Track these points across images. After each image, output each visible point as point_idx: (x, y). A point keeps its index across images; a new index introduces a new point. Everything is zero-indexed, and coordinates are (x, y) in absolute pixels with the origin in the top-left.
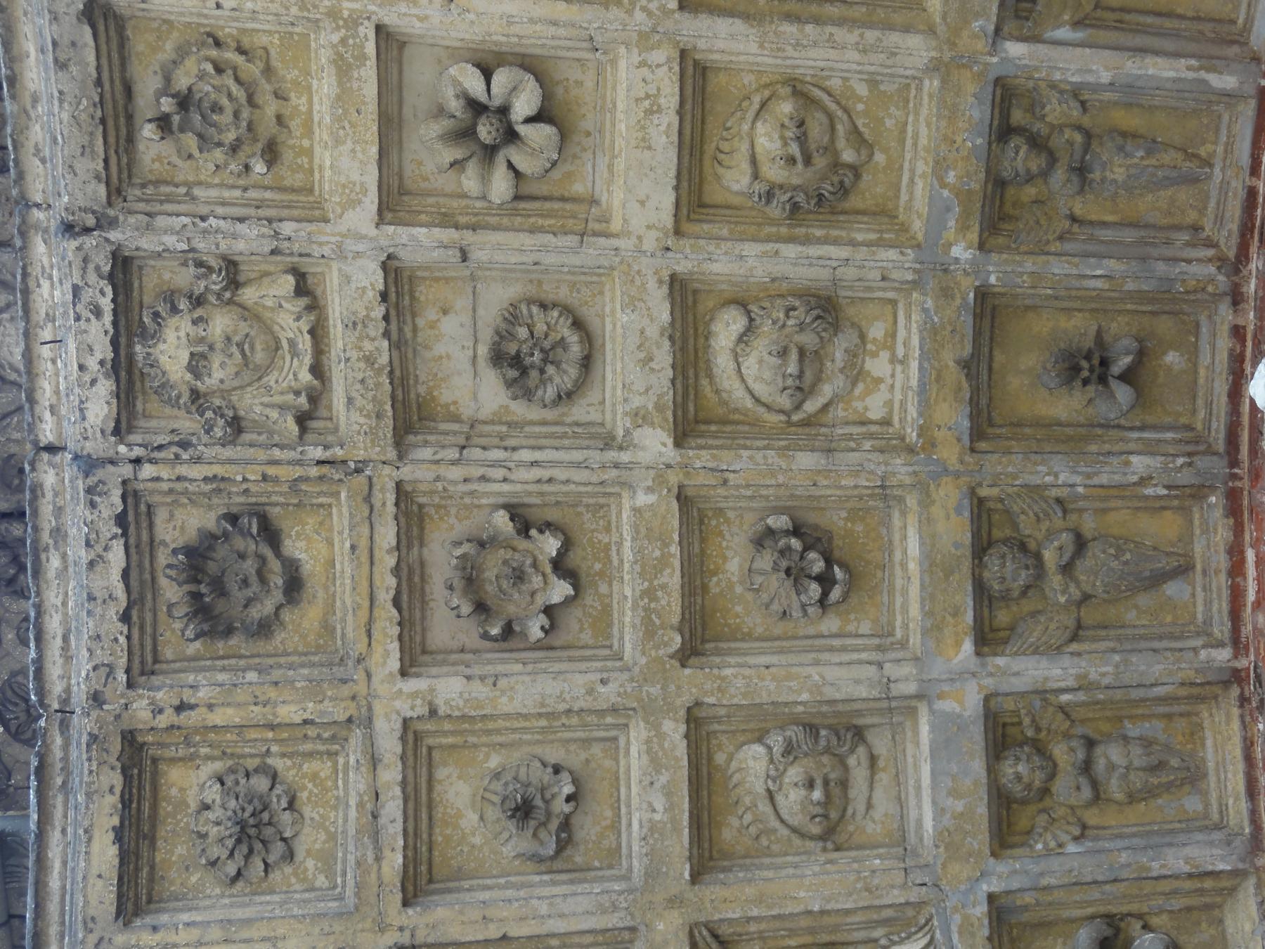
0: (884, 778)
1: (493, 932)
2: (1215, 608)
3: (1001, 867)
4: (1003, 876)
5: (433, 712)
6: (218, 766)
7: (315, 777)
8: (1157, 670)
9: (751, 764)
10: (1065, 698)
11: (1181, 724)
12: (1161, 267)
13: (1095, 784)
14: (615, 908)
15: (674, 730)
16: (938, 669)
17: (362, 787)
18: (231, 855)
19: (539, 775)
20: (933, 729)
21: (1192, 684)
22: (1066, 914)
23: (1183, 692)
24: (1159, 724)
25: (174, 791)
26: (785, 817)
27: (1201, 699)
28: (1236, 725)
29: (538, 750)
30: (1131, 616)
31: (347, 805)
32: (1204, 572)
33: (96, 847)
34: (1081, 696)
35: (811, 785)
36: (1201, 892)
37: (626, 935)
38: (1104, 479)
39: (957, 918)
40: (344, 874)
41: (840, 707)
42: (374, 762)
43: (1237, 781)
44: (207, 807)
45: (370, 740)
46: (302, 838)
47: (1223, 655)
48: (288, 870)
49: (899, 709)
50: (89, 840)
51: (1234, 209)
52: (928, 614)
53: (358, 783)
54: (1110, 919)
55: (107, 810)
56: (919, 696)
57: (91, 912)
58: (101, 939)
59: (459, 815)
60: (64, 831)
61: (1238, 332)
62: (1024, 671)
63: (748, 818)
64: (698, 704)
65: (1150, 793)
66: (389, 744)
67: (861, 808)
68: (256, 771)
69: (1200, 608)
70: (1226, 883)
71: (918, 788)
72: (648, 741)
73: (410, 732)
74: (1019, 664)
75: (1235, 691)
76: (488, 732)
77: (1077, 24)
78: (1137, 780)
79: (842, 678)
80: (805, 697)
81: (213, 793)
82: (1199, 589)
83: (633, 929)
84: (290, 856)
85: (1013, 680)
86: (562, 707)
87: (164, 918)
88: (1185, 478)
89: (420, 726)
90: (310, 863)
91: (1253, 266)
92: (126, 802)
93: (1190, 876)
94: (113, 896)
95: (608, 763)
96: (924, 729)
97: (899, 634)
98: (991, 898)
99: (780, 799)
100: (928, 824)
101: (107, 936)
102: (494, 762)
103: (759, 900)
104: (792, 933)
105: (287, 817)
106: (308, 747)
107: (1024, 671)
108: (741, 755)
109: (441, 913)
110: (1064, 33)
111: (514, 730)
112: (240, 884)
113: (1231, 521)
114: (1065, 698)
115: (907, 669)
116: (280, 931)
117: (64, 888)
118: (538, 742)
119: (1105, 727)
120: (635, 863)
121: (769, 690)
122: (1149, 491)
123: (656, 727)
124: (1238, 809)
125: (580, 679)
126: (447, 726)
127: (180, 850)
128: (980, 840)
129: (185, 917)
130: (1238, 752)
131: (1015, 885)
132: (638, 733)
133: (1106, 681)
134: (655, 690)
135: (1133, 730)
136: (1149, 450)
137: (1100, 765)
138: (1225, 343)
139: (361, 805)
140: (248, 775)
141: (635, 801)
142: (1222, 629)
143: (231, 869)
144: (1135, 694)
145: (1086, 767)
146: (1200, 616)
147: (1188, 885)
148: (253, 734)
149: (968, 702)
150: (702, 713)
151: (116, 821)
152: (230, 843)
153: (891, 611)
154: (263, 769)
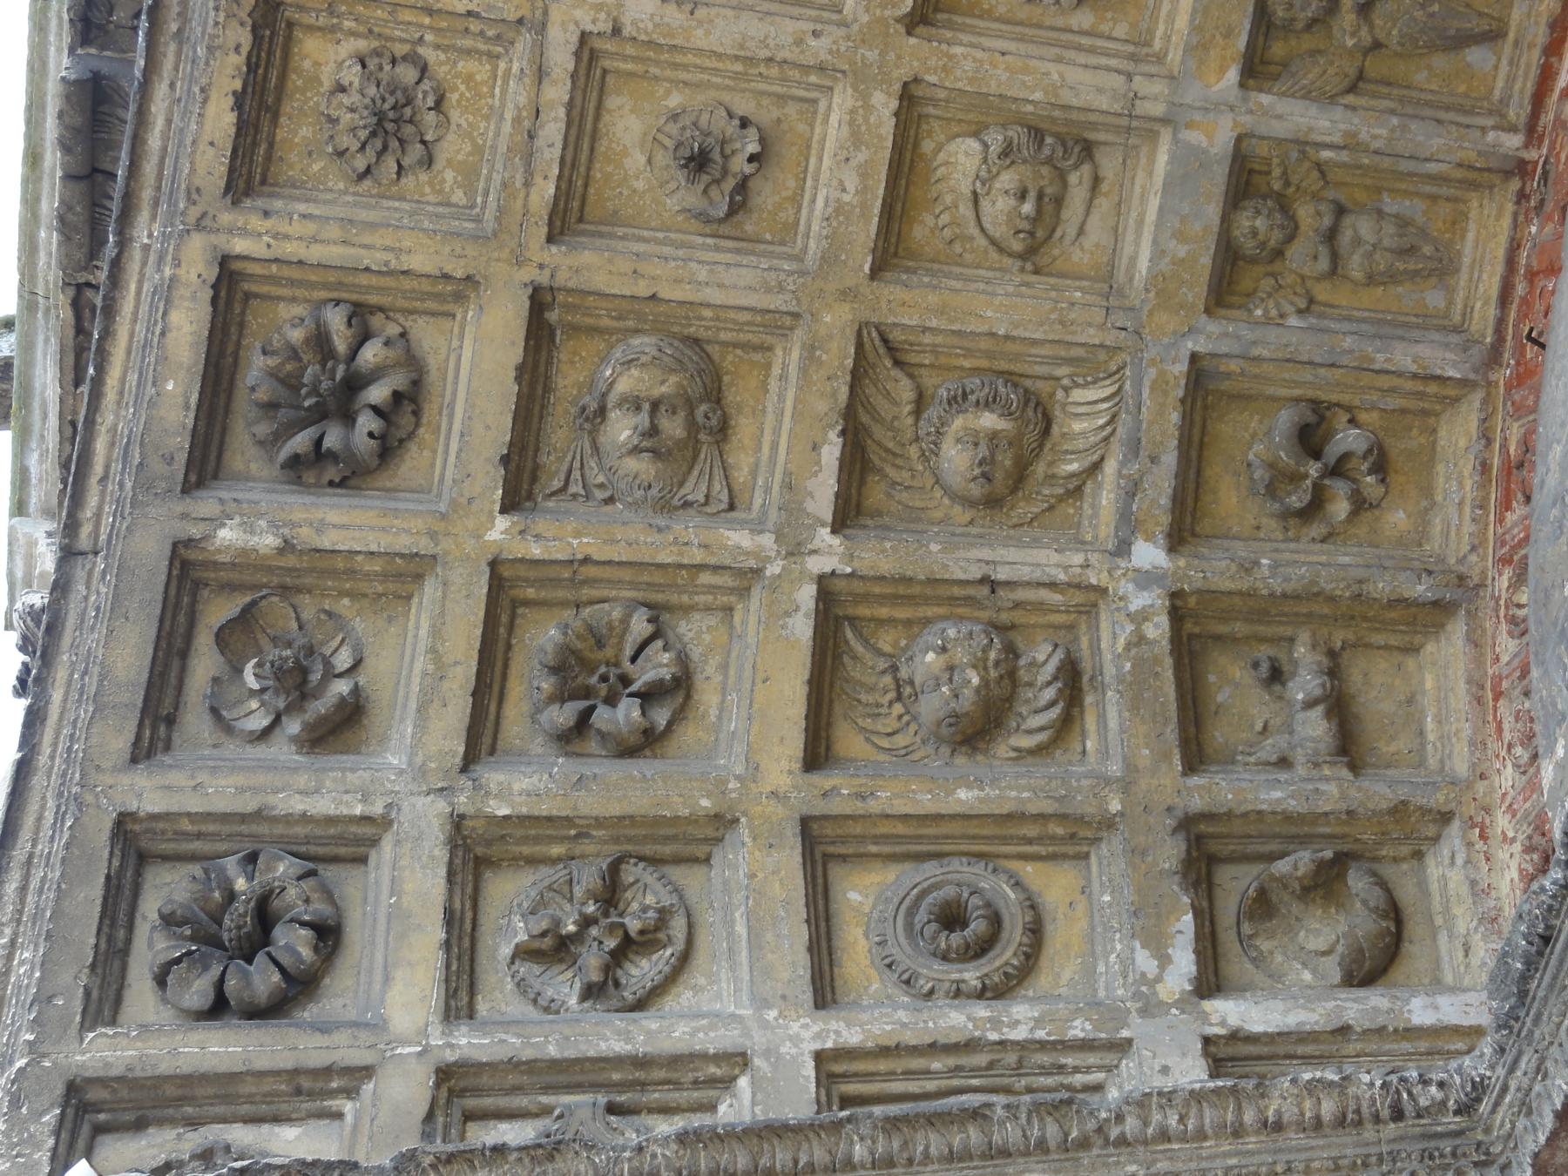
0: (1103, 204)
1: (642, 289)
2: (1517, 87)
3: (1213, 327)
4: (1213, 336)
5: (616, 31)
6: (362, 45)
7: (469, 78)
8: (1437, 144)
9: (959, 159)
11: (1445, 209)
13: (1335, 257)
14: (781, 288)
15: (884, 105)
16: (1192, 94)
17: (522, 100)
18: (363, 147)
19: (722, 125)
20: (1173, 159)
21: (1471, 167)
22: (1270, 391)
23: (1459, 174)
24: (1420, 205)
25: (307, 64)
26: (987, 225)
27: (1474, 186)
28: (1506, 222)
29: (726, 97)
30: (1420, 77)
31: (502, 117)
32: (1516, 43)
33: (211, 109)
34: (1344, 156)
35: (1022, 196)
36: (1421, 395)
37: (788, 321)
39: (1152, 373)
40: (486, 194)
41: (1074, 116)
42: (541, 74)
43: (1491, 284)
44: (342, 89)
45: (540, 49)
46: (444, 144)
47: (1512, 142)
48: (424, 177)
49: (1138, 129)
50: (205, 101)
52: (1196, 29)
53: (518, 94)
54: (1316, 405)
55: (230, 71)
56: (1165, 121)
57: (197, 182)
58: (204, 215)
59: (625, 153)
60: (172, 85)
62: (1288, 115)
63: (945, 218)
64: (916, 80)
65: (1392, 278)
66: (561, 59)
67: (1072, 232)
68: (404, 58)
69: (1500, 84)
70: (1452, 392)
71: (1140, 223)
72: (852, 112)
73: (586, 50)
74: (1284, 106)
75: (1515, 184)
76: (675, 66)
78: (1382, 261)
79: (1085, 85)
80: (1038, 96)
81: (352, 75)
82: (1504, 62)
83: (796, 316)
84: (428, 161)
85: (1274, 122)
86: (764, 53)
87: (278, 204)
89: (598, 44)
90: (449, 175)
92: (252, 66)
93: (1415, 376)
94: (224, 169)
95: (802, 127)
96: (1162, 158)
97: (1157, 44)
98: (1194, 358)
99: (985, 204)
100: (1143, 264)
101: (211, 212)
102: (675, 101)
103: (941, 311)
104: (969, 353)
105: (431, 117)
106: (467, 43)
107: (1288, 115)
108: (952, 147)
109: (587, 257)
111: (704, 69)
112: (367, 183)
114: (1326, 154)
115: (1158, 87)
116: (407, 244)
117: (164, 149)
118: (728, 88)
119: (1360, 196)
120: (812, 244)
121: (999, 79)
123: (865, 97)
124: (1484, 316)
125: (790, 26)
126: (630, 50)
127: (305, 132)
128: (1196, 292)
129: (302, 207)
130: (1501, 253)
131: (1224, 349)
132: (842, 100)
133: (1376, 145)
134: (872, 55)
135: (1390, 205)
137: (1346, 237)
139: (517, 120)
140: (394, 62)
141: (825, 175)
142: (1518, 111)
143: (360, 164)
144: (1406, 166)
145: (1331, 236)
146: (1497, 94)
147: (1409, 385)
148: (407, 16)
149: (1218, 138)
150: (919, 91)
151: (238, 85)
152: (363, 134)
153: (1154, 17)
154: (412, 58)
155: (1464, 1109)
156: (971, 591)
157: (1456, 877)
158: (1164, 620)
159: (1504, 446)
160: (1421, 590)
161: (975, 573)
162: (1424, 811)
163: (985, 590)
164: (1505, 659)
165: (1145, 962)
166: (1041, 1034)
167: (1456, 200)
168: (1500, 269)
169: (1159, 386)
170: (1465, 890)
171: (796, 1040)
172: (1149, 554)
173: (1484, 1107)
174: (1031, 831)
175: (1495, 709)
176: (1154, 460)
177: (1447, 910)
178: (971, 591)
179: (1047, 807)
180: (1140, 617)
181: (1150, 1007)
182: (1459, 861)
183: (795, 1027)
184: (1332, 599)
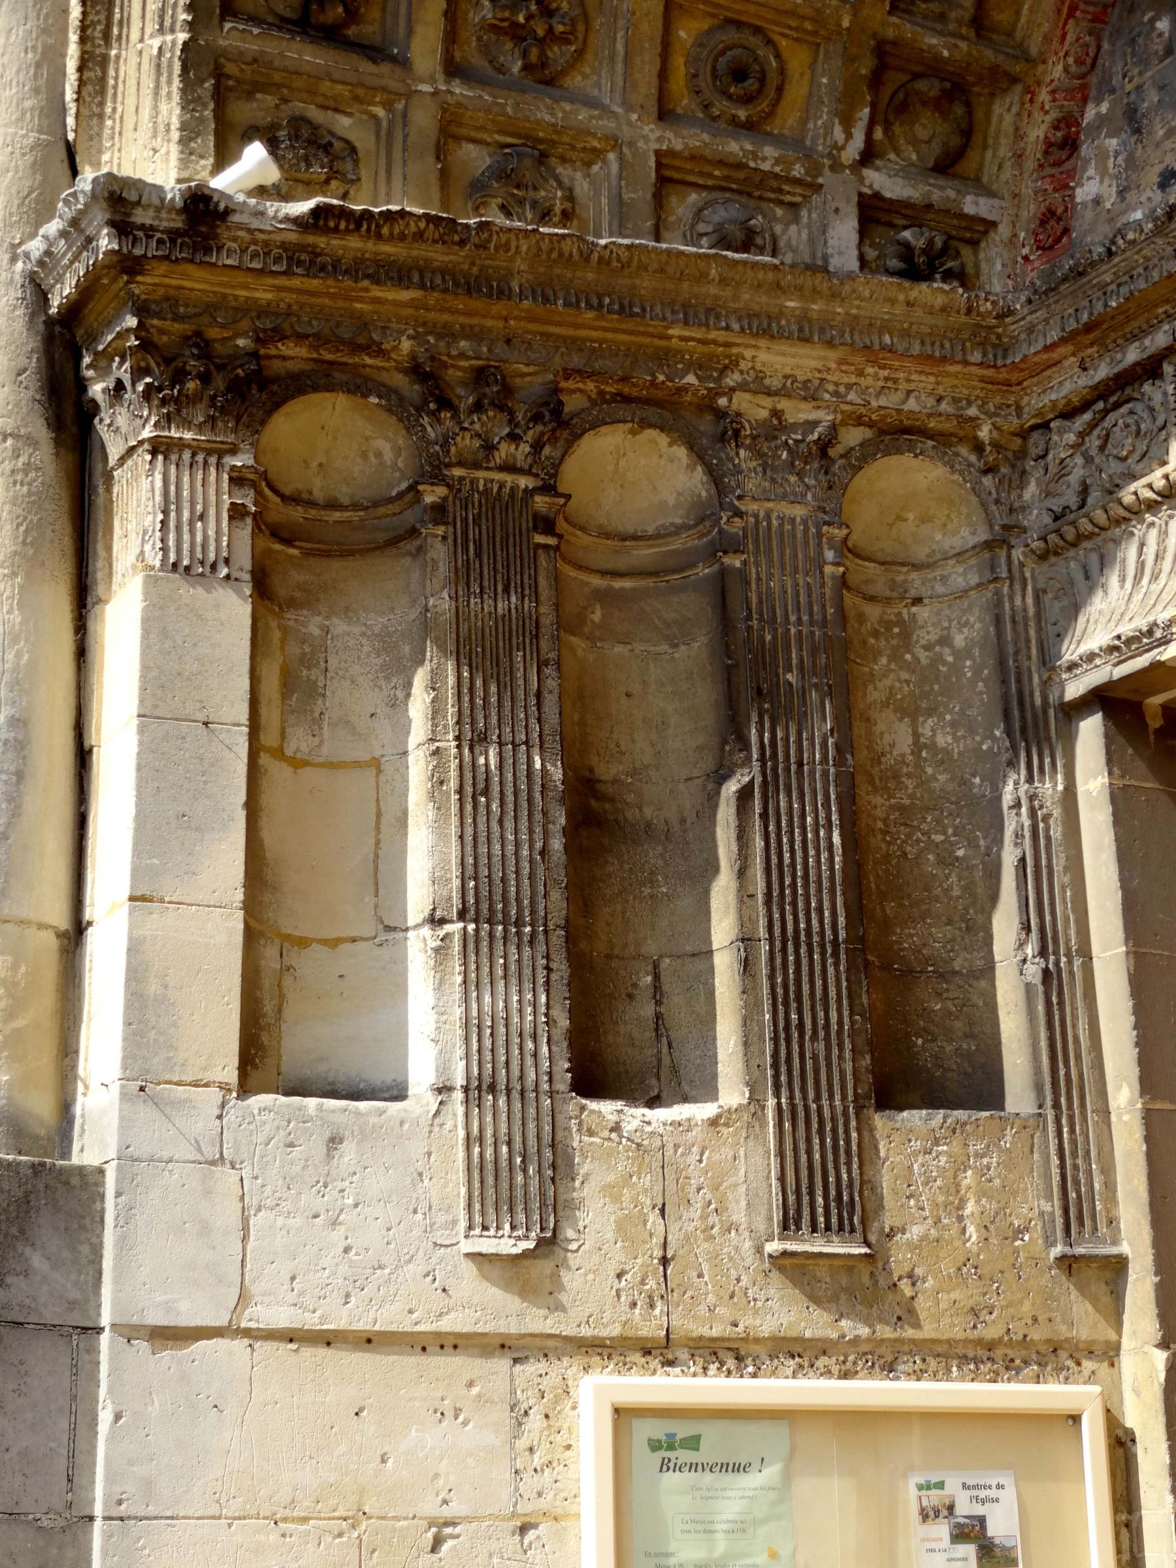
155: (999, 317)
157: (1008, 119)
162: (1006, 74)
165: (839, 134)
166: (777, 169)
170: (1011, 130)
171: (646, 139)
173: (1007, 320)
175: (1065, 24)
177: (997, 137)
181: (836, 167)
182: (1014, 110)
183: (646, 129)
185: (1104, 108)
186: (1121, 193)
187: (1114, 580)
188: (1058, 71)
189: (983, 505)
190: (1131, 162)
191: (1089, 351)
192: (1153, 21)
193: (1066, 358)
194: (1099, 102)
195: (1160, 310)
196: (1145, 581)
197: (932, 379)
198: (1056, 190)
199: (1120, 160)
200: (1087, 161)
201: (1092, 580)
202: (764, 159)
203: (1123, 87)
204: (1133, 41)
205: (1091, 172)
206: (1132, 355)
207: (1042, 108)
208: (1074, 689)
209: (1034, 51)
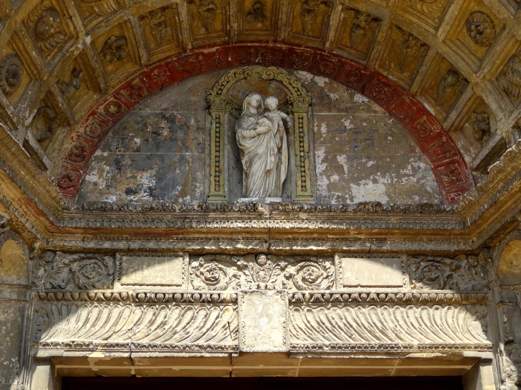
2: (200, 41)
3: (136, 19)
10: (177, 18)
12: (284, 28)
21: (183, 43)
28: (173, 53)
30: (196, 22)
36: (135, 57)
38: (231, 18)
39: (123, 14)
43: (161, 56)
51: (297, 41)
61: (267, 42)
70: (138, 62)
75: (181, 51)
77: (344, 18)
85: (181, 8)
88: (232, 34)
91: (283, 46)
93: (139, 56)
110: (343, 15)
113: (222, 44)
122: (228, 26)
124: (155, 58)
133: (182, 26)
136: (239, 26)
138: (264, 38)
144: (179, 32)
147: (137, 55)
156: (67, 14)
157: (61, 136)
158: (78, 52)
159: (133, 80)
160: (102, 86)
161: (71, 14)
162: (69, 122)
163: (68, 17)
164: (99, 111)
167: (174, 39)
168: (164, 57)
169: (122, 17)
170: (61, 140)
172: (88, 40)
173: (65, 211)
174: (32, 68)
175: (89, 116)
176: (106, 26)
177: (55, 140)
178: (67, 14)
179: (40, 69)
180: (77, 48)
181: (23, 125)
182: (64, 134)
184: (94, 73)
185: (105, 154)
186: (108, 187)
187: (73, 319)
188: (82, 130)
189: (28, 271)
190: (114, 178)
191: (89, 236)
192: (133, 137)
193: (78, 233)
194: (103, 150)
195: (125, 236)
196: (88, 326)
197: (34, 219)
198: (72, 170)
199: (109, 175)
200: (93, 169)
201: (62, 316)
202: (10, 110)
203: (115, 152)
204: (123, 139)
205: (95, 172)
206: (107, 245)
207: (72, 138)
208: (42, 353)
209: (77, 119)
